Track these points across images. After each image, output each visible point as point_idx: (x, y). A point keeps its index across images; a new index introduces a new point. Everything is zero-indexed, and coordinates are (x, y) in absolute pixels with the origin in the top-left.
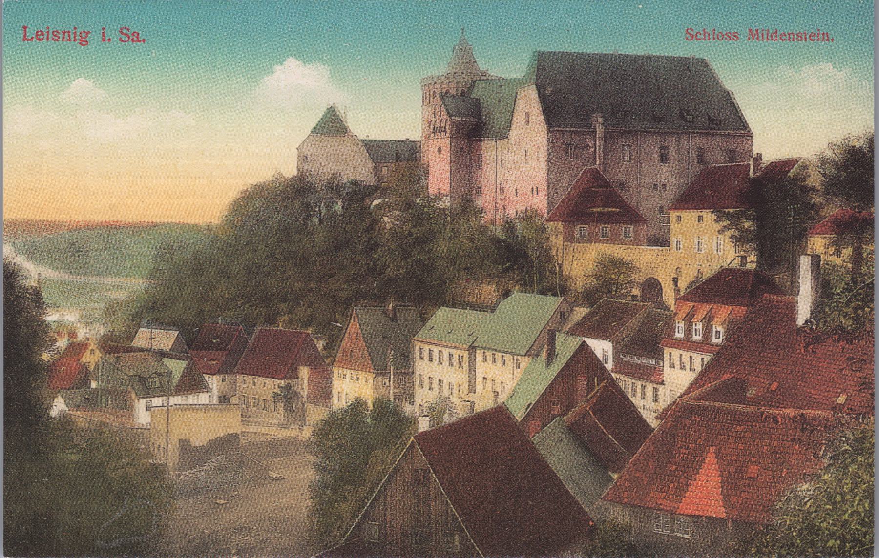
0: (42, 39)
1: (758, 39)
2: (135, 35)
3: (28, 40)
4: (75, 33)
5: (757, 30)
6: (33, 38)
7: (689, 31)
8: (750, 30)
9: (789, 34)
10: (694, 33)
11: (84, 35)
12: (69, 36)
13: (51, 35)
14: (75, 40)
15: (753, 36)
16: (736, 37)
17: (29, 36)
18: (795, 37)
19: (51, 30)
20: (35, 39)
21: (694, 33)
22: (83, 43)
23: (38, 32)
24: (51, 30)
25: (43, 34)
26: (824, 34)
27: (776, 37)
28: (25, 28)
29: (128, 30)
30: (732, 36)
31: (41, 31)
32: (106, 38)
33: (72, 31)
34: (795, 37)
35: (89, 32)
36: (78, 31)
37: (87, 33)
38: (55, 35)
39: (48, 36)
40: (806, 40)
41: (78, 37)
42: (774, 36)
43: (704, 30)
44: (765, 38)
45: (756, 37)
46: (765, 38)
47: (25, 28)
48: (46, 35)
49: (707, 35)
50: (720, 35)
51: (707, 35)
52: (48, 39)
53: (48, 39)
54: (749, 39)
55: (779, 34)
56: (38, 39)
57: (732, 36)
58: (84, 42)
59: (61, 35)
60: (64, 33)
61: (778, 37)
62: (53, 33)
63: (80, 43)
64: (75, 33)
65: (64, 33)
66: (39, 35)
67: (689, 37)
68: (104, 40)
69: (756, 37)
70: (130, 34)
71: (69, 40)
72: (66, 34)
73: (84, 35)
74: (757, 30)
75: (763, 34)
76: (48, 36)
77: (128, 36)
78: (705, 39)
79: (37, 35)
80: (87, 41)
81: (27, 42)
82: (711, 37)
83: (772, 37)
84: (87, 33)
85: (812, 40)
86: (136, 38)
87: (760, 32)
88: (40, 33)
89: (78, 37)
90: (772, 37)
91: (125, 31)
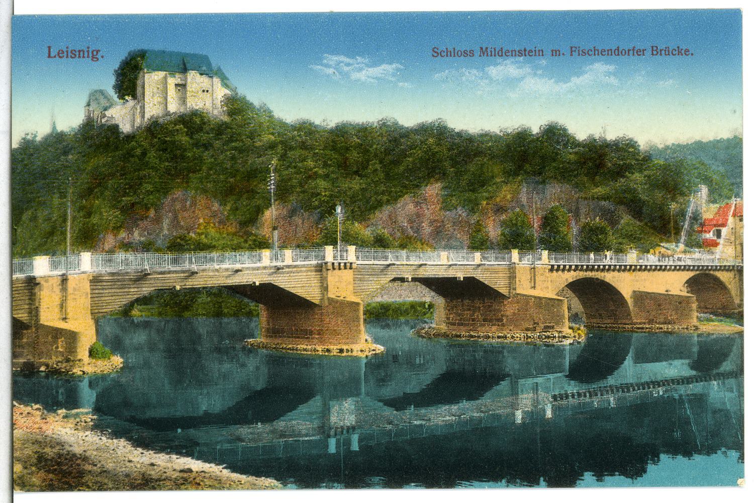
1: (487, 56)
4: (88, 52)
5: (487, 48)
7: (436, 50)
8: (482, 48)
9: (512, 51)
10: (439, 52)
11: (95, 53)
13: (70, 54)
14: (88, 57)
15: (484, 54)
16: (471, 53)
17: (52, 55)
18: (517, 53)
19: (70, 50)
21: (439, 52)
22: (95, 59)
24: (70, 50)
26: (539, 51)
27: (502, 52)
28: (49, 48)
30: (469, 54)
33: (86, 50)
34: (517, 53)
35: (99, 51)
36: (90, 50)
37: (98, 51)
38: (73, 54)
39: (67, 55)
40: (525, 56)
41: (91, 55)
42: (500, 54)
43: (447, 49)
44: (493, 53)
45: (486, 54)
46: (493, 53)
47: (49, 48)
48: (65, 53)
49: (449, 53)
50: (459, 52)
51: (449, 53)
52: (67, 57)
54: (480, 56)
55: (504, 51)
56: (60, 57)
57: (469, 54)
58: (94, 58)
59: (77, 53)
61: (504, 54)
63: (92, 60)
64: (88, 52)
65: (79, 51)
66: (60, 54)
67: (435, 55)
69: (486, 54)
71: (84, 57)
72: (81, 53)
73: (95, 53)
74: (487, 48)
75: (491, 51)
76: (67, 55)
78: (447, 56)
79: (59, 53)
80: (96, 58)
81: (50, 59)
82: (453, 55)
83: (498, 52)
84: (98, 51)
85: (530, 56)
87: (489, 50)
88: (61, 52)
90: (498, 52)
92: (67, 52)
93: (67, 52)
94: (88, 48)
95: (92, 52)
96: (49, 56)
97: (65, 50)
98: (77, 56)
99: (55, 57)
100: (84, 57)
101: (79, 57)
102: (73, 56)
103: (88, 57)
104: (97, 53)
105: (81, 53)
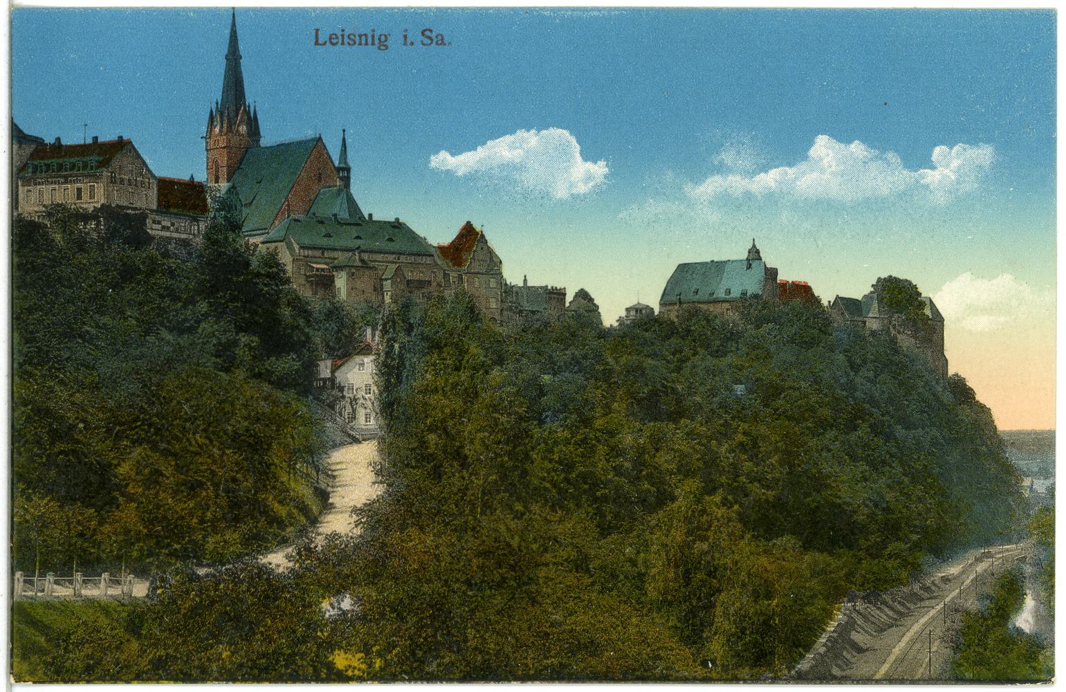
0: (337, 43)
2: (440, 37)
3: (320, 45)
6: (325, 43)
11: (383, 38)
12: (366, 40)
13: (346, 40)
14: (373, 44)
17: (321, 41)
20: (328, 43)
22: (382, 48)
23: (333, 34)
25: (337, 38)
28: (317, 30)
29: (431, 31)
31: (336, 35)
32: (409, 42)
38: (353, 40)
39: (343, 40)
41: (377, 41)
47: (317, 30)
48: (340, 38)
53: (343, 43)
56: (334, 44)
59: (357, 38)
60: (360, 36)
62: (349, 37)
63: (379, 48)
65: (360, 36)
68: (405, 44)
70: (433, 35)
71: (366, 44)
72: (363, 38)
73: (383, 38)
76: (343, 40)
77: (430, 38)
79: (330, 38)
81: (319, 46)
86: (441, 41)
89: (377, 41)
91: (427, 33)
92: (343, 36)
93: (343, 36)
94: (373, 31)
95: (379, 39)
96: (317, 43)
97: (339, 34)
98: (357, 42)
99: (325, 43)
100: (366, 44)
101: (360, 44)
102: (351, 42)
103: (373, 44)
104: (386, 41)
105: (363, 38)
